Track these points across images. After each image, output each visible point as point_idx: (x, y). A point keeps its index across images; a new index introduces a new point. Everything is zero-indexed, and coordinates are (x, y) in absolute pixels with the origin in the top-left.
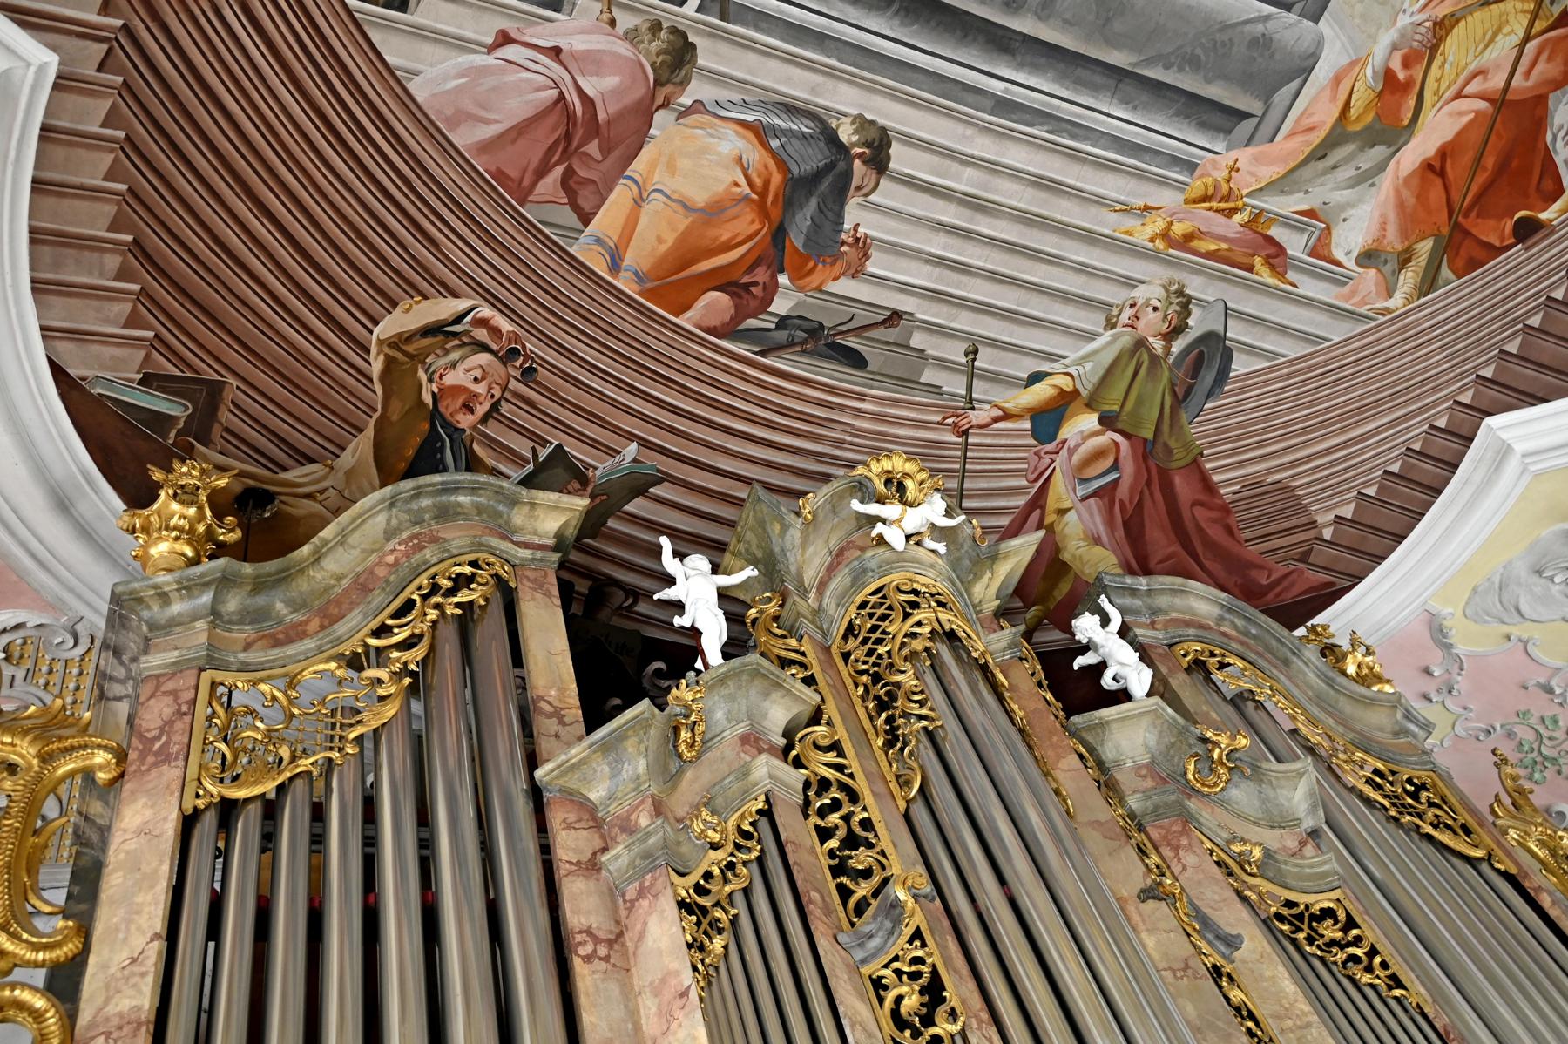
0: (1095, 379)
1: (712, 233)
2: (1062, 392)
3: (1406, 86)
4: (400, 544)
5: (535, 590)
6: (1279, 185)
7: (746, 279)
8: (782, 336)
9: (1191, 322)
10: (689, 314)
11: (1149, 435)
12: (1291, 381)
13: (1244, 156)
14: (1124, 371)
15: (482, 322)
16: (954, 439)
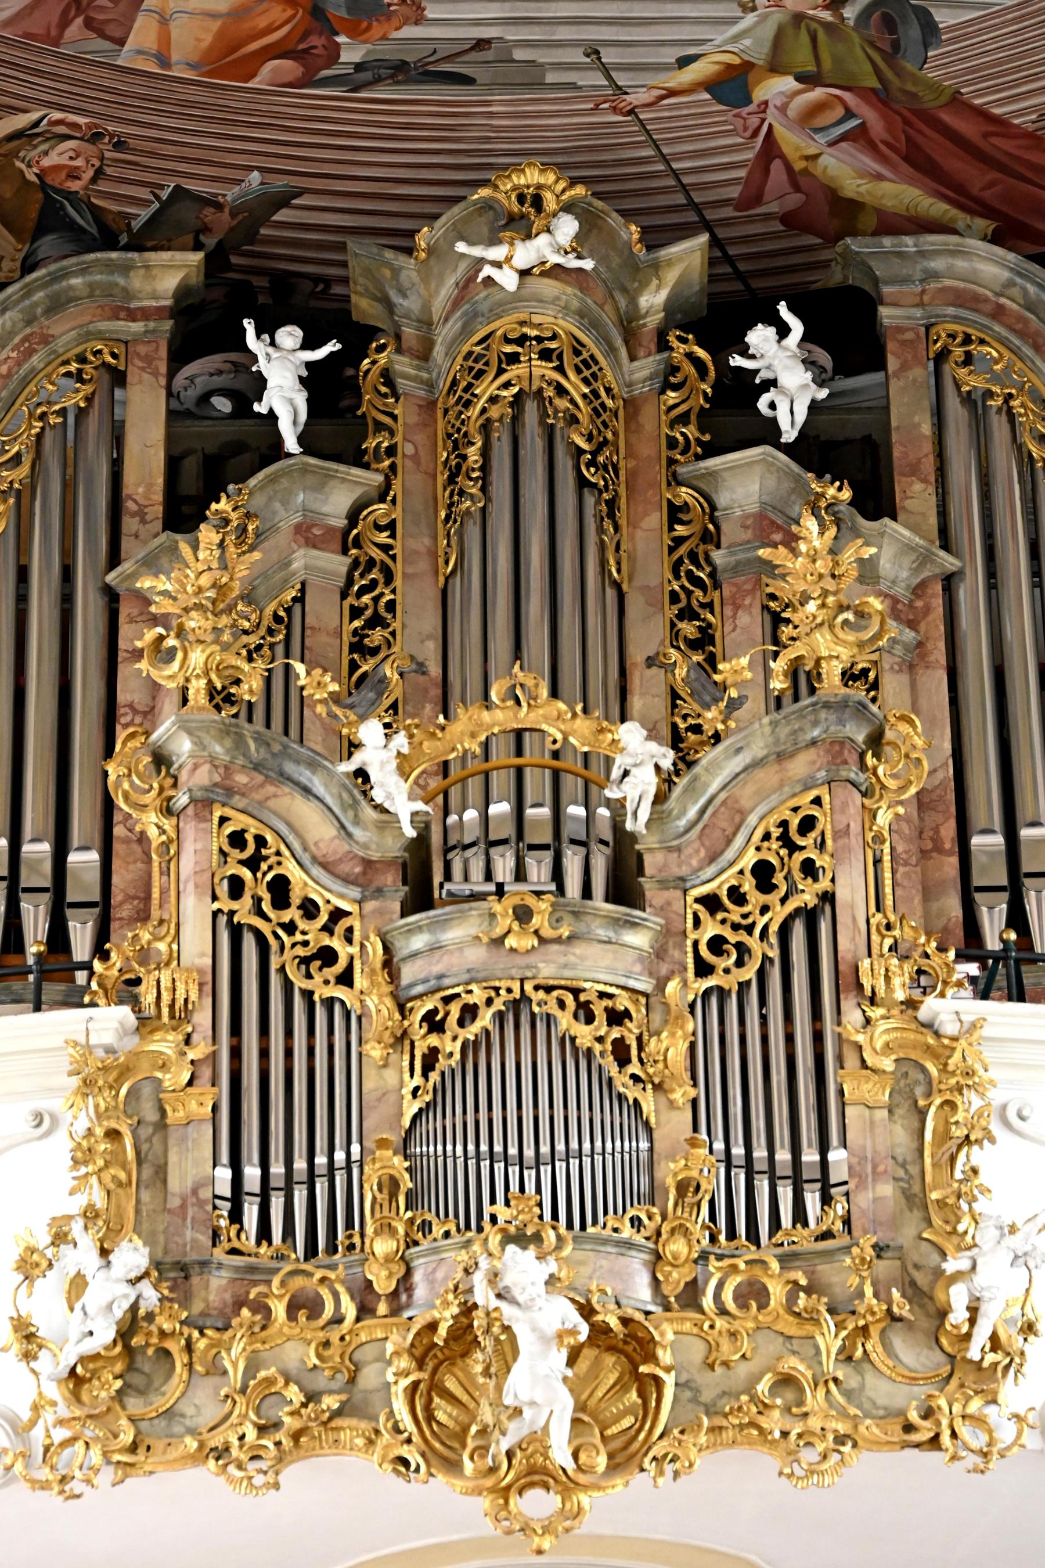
0: (766, 48)
2: (729, 67)
4: (13, 350)
5: (143, 369)
7: (301, 47)
10: (257, 79)
11: (874, 83)
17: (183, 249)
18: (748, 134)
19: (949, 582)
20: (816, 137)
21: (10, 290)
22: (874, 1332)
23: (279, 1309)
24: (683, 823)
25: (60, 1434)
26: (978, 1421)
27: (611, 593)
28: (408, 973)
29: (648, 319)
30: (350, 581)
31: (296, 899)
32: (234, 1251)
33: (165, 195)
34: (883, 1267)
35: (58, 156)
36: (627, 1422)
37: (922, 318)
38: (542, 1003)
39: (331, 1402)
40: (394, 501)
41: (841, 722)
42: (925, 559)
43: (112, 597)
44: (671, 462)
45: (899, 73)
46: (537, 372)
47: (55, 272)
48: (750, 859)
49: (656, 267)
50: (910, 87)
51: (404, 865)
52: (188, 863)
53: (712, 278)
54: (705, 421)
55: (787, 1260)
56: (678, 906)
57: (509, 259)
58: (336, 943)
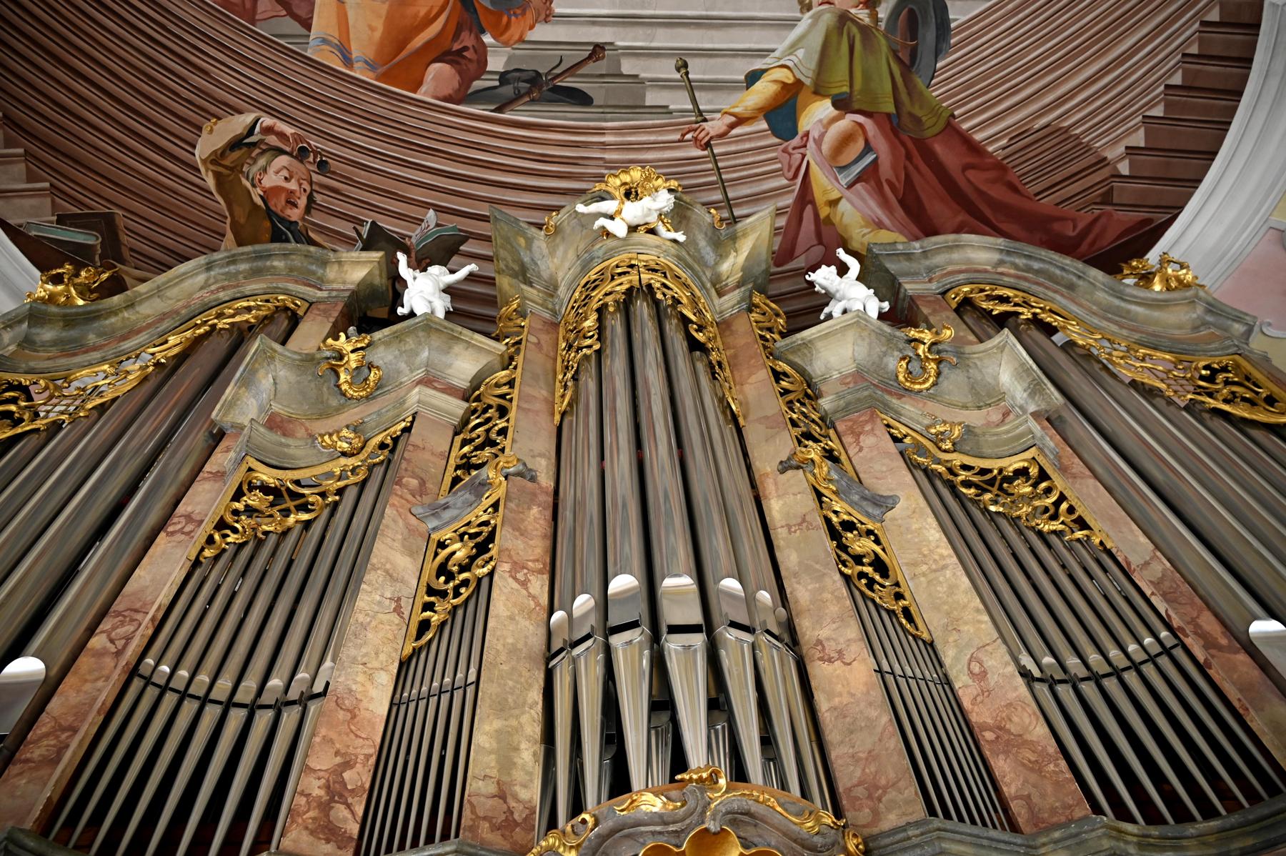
0: (813, 65)
1: (411, 11)
2: (785, 86)
7: (456, 47)
8: (508, 90)
10: (423, 89)
11: (890, 108)
12: (1021, 16)
14: (838, 50)
15: (269, 130)
16: (700, 153)
18: (791, 174)
20: (839, 177)
29: (730, 280)
30: (465, 422)
33: (365, 231)
37: (938, 288)
40: (515, 368)
45: (911, 91)
47: (260, 252)
49: (734, 238)
50: (918, 112)
57: (619, 212)
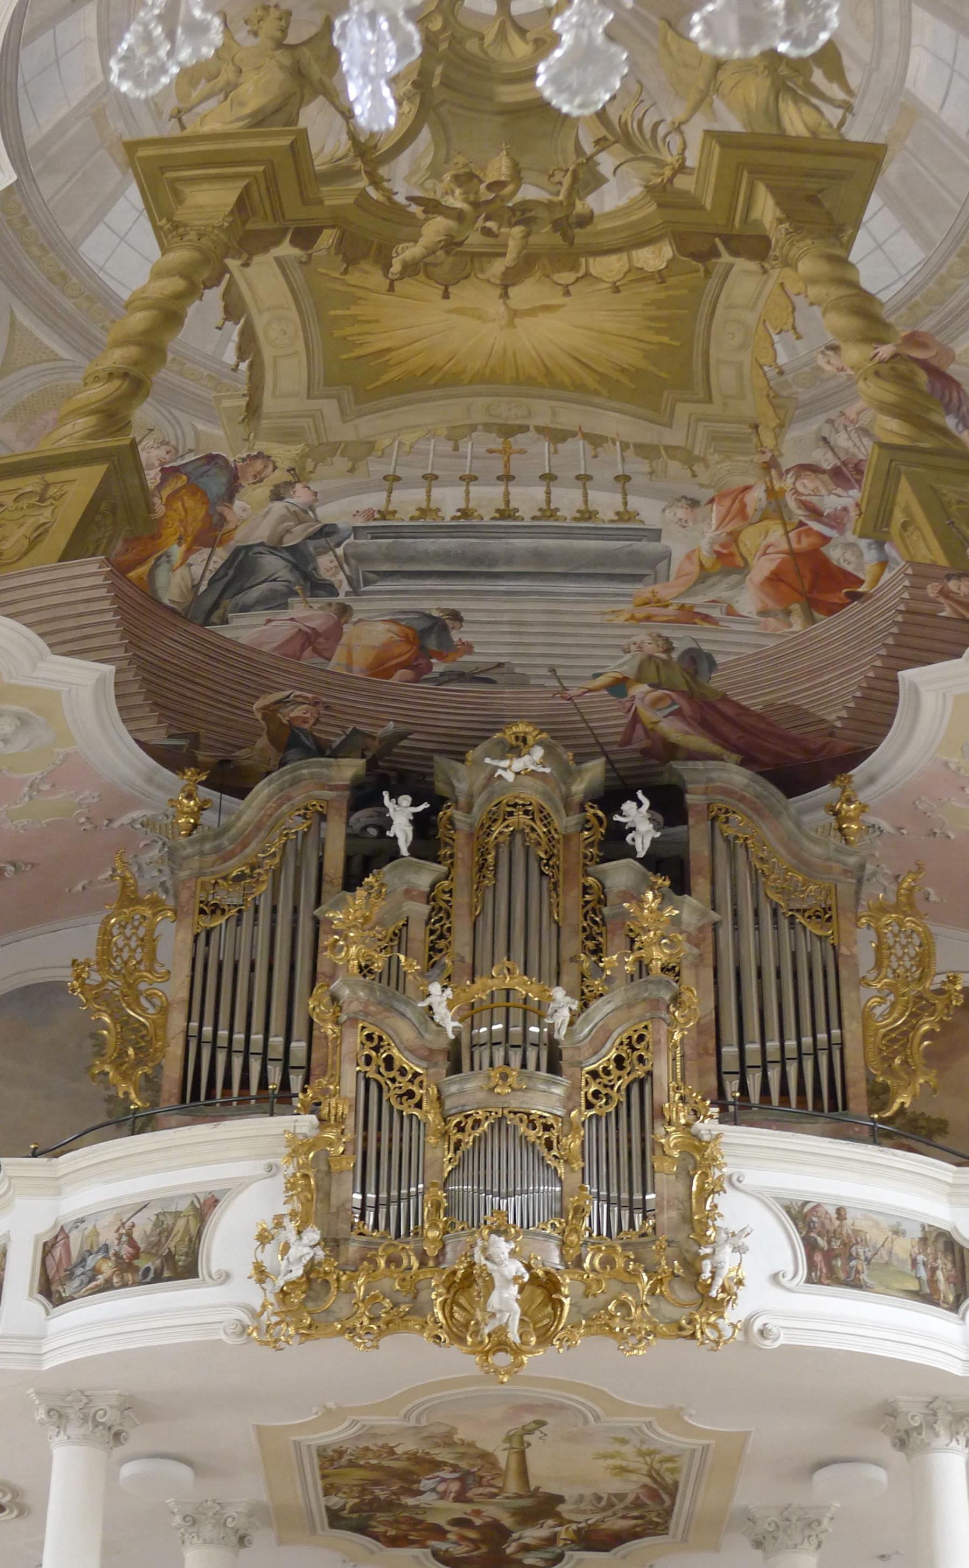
0: (635, 669)
3: (731, 555)
6: (689, 592)
9: (675, 645)
13: (657, 587)
17: (357, 757)
19: (715, 926)
21: (273, 774)
22: (666, 1281)
23: (382, 1262)
24: (582, 1035)
25: (274, 1319)
26: (714, 1326)
27: (554, 927)
28: (448, 1103)
30: (430, 918)
31: (397, 1064)
32: (361, 1234)
33: (348, 732)
34: (670, 1251)
35: (298, 712)
36: (545, 1322)
38: (511, 1120)
39: (405, 1308)
41: (659, 990)
42: (703, 915)
43: (317, 922)
44: (585, 865)
46: (522, 821)
48: (613, 1054)
49: (580, 772)
51: (449, 1053)
52: (345, 1048)
53: (607, 778)
54: (601, 845)
55: (625, 1246)
56: (578, 1075)
57: (510, 767)
58: (415, 1089)
